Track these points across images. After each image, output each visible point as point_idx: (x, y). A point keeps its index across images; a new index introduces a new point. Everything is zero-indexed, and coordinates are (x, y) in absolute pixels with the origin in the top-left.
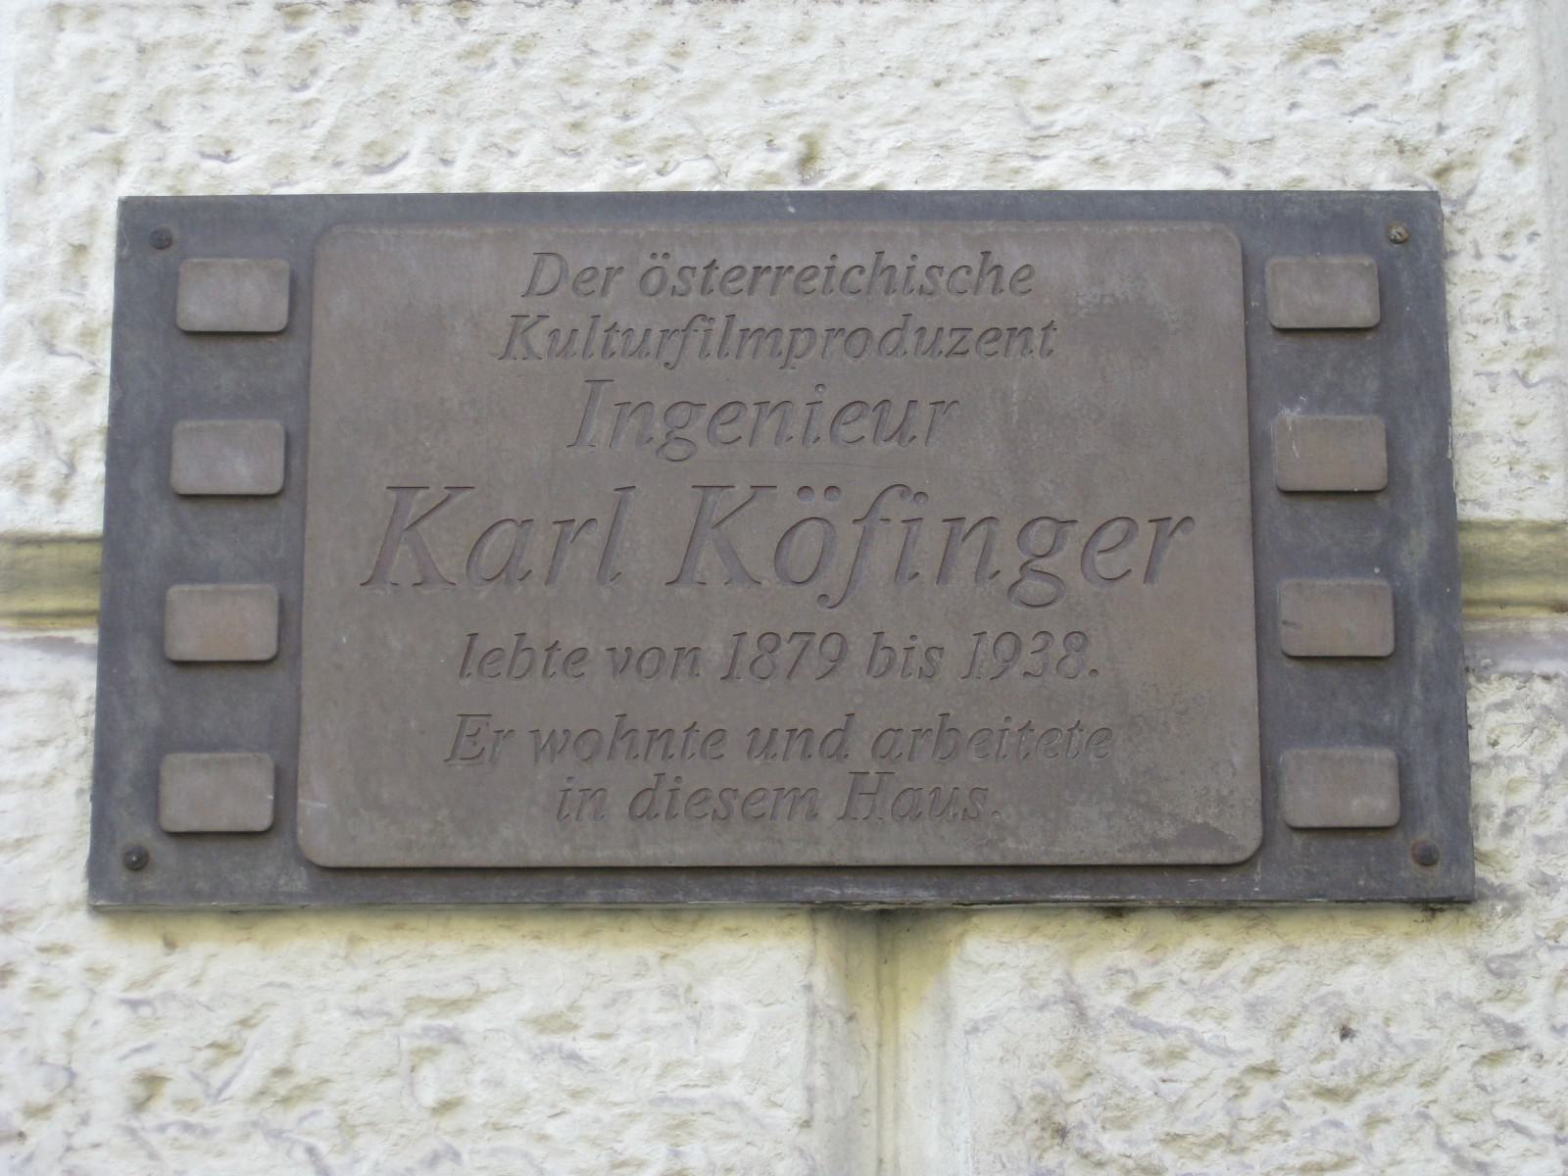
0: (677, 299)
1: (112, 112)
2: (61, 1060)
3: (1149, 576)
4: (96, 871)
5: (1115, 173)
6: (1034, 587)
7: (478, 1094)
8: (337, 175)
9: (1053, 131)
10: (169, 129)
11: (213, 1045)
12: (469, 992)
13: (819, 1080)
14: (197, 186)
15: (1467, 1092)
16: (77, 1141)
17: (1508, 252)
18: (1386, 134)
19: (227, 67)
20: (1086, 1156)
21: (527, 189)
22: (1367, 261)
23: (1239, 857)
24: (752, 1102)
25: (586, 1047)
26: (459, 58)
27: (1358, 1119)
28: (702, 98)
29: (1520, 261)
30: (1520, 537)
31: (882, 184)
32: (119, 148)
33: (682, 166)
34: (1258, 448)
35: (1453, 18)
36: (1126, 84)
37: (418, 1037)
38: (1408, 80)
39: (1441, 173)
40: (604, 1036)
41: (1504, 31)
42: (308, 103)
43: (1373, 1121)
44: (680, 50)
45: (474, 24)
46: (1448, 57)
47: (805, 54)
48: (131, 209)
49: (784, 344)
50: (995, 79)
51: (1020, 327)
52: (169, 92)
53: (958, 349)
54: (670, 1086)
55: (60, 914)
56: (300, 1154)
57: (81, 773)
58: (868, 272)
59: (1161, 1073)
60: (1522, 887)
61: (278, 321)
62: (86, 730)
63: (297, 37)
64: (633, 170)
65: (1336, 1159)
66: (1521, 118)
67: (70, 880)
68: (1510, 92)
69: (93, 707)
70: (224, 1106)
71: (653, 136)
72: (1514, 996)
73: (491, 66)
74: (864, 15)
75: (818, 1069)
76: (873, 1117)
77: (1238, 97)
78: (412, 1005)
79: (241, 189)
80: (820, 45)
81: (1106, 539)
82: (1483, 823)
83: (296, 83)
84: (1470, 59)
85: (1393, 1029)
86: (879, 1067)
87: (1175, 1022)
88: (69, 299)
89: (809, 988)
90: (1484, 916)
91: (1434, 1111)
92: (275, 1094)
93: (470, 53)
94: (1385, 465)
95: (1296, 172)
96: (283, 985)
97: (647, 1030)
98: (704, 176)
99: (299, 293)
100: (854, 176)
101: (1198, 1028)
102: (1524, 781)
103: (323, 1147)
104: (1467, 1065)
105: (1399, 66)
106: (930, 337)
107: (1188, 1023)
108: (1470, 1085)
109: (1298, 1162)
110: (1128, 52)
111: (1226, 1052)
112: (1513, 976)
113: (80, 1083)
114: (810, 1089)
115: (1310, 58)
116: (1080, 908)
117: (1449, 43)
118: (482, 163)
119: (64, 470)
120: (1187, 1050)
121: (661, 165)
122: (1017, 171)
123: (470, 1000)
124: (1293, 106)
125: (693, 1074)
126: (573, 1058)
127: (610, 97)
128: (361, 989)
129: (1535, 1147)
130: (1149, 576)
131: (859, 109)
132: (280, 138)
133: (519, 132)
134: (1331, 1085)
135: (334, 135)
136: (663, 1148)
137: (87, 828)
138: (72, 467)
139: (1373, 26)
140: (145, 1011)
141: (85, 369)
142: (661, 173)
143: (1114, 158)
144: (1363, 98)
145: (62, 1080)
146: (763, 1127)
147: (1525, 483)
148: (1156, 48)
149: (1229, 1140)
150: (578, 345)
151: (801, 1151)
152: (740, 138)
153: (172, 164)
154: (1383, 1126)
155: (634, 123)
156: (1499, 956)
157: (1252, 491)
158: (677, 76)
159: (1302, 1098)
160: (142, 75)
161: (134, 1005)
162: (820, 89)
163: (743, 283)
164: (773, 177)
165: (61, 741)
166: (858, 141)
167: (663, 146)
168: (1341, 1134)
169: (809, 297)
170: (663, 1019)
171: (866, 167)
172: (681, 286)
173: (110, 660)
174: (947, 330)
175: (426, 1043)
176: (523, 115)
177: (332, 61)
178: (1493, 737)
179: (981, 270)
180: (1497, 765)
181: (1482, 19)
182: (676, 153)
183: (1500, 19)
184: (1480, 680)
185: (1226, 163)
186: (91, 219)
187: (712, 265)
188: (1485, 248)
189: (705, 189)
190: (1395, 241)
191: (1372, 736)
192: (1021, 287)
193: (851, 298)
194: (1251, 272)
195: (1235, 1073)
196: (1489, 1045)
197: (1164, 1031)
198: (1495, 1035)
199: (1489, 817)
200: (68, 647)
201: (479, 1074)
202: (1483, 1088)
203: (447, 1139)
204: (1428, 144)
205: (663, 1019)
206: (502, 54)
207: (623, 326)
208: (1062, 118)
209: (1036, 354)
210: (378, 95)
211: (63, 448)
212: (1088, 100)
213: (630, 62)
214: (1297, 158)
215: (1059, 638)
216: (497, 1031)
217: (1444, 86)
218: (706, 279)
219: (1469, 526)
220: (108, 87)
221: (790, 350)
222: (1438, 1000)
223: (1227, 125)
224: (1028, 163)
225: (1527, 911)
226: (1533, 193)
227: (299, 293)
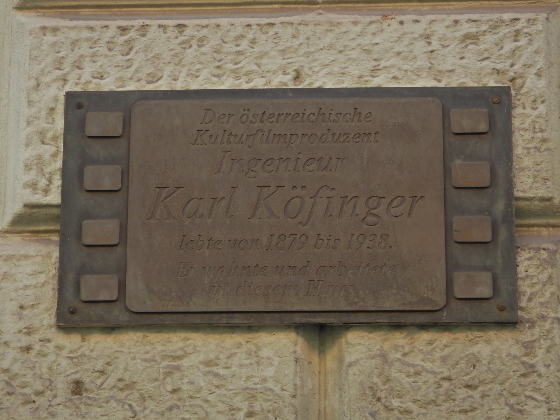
8: (138, 84)
28: (261, 57)
31: (321, 86)
44: (253, 41)
47: (297, 42)
64: (238, 82)
71: (245, 70)
74: (316, 29)
80: (301, 39)
98: (262, 83)
100: (312, 83)
118: (187, 80)
122: (367, 81)
127: (230, 57)
131: (314, 61)
141: (54, 149)
142: (247, 82)
164: (285, 84)
166: (313, 72)
171: (316, 80)
172: (253, 120)
176: (201, 63)
182: (252, 76)
189: (262, 88)
193: (310, 124)
208: (383, 63)
211: (47, 176)
213: (237, 45)
218: (262, 117)
224: (371, 78)
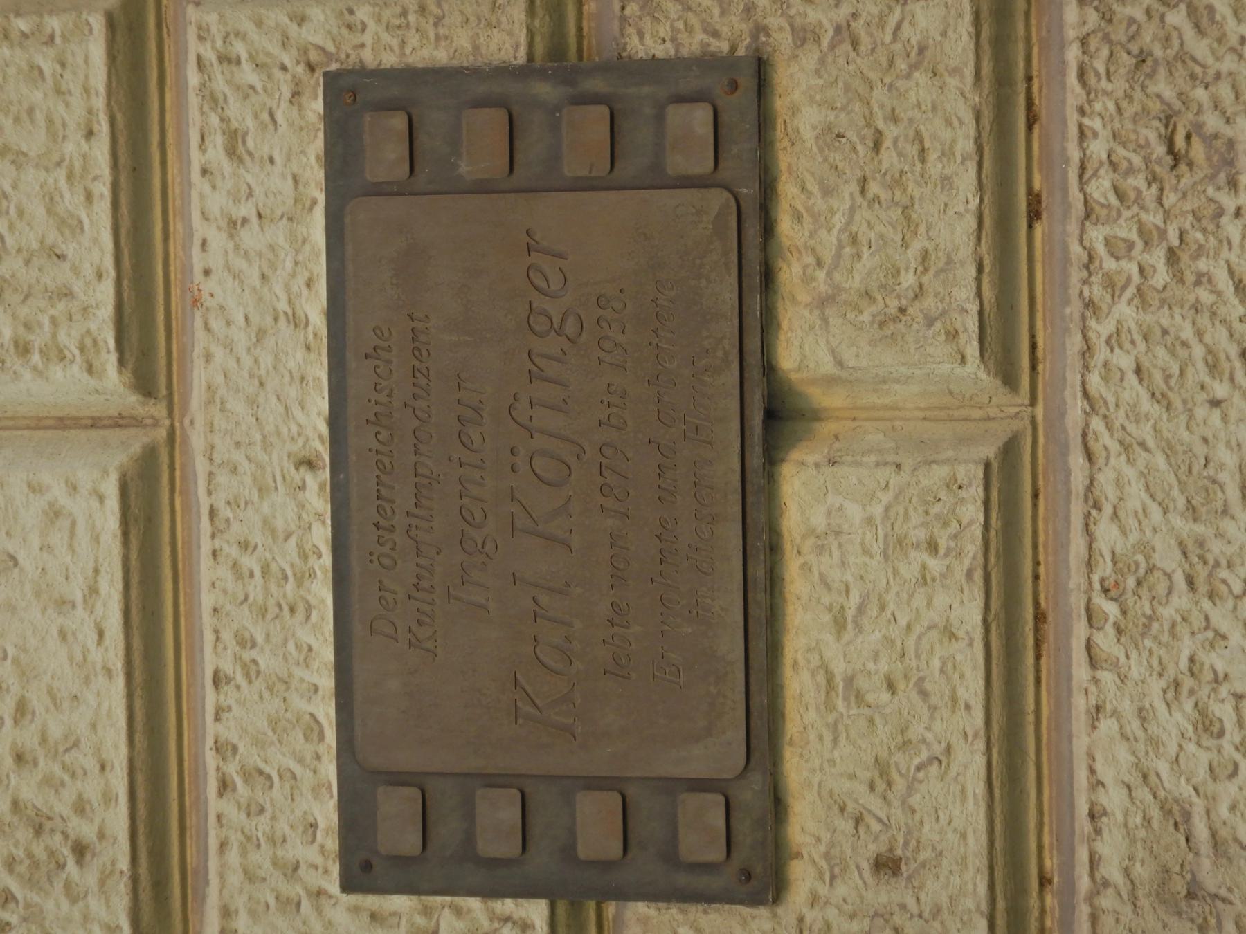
0: (397, 547)
1: (288, 899)
2: (867, 921)
3: (561, 256)
4: (755, 900)
5: (315, 274)
6: (571, 327)
7: (884, 666)
8: (325, 759)
9: (290, 313)
10: (298, 862)
11: (856, 829)
12: (822, 672)
13: (873, 458)
14: (333, 844)
15: (875, 60)
16: (915, 911)
17: (359, 27)
18: (288, 104)
19: (260, 826)
20: (916, 296)
21: (331, 639)
22: (368, 118)
23: (733, 203)
24: (886, 498)
25: (855, 599)
26: (250, 682)
27: (893, 128)
28: (273, 532)
29: (365, 19)
30: (537, 23)
31: (325, 419)
32: (309, 893)
33: (316, 543)
34: (483, 188)
35: (214, 59)
36: (260, 267)
37: (849, 704)
38: (252, 87)
39: (311, 68)
40: (847, 591)
41: (221, 27)
42: (281, 777)
43: (894, 118)
44: (244, 546)
45: (230, 673)
46: (238, 62)
47: (245, 466)
48: (348, 886)
49: (426, 481)
50: (259, 350)
51: (412, 335)
52: (275, 863)
53: (426, 374)
54: (877, 548)
55: (779, 923)
56: (921, 775)
57: (695, 911)
58: (378, 429)
59: (865, 249)
60: (751, 24)
61: (414, 792)
62: (668, 908)
63: (239, 781)
64: (319, 573)
65: (917, 142)
66: (277, 17)
67: (761, 915)
68: (259, 24)
69: (653, 905)
70: (893, 822)
71: (297, 561)
72: (817, 30)
73: (254, 662)
74: (220, 430)
75: (866, 459)
76: (897, 423)
77: (266, 196)
78: (830, 707)
79: (335, 818)
80: (238, 457)
81: (541, 283)
82: (712, 48)
83: (268, 784)
84: (239, 48)
85: (839, 105)
86: (867, 420)
87: (834, 240)
88: (403, 922)
89: (817, 465)
90: (769, 49)
91: (887, 80)
92: (885, 790)
93: (247, 676)
94: (493, 109)
95: (313, 159)
96: (819, 785)
97: (843, 563)
98: (322, 529)
99: (397, 779)
100: (321, 437)
101: (838, 226)
102: (686, 23)
103: (916, 761)
104: (859, 60)
105: (247, 92)
106: (417, 391)
107: (835, 231)
108: (871, 58)
109: (919, 165)
110: (239, 263)
111: (852, 210)
112: (805, 30)
113: (881, 910)
114: (877, 464)
115: (241, 149)
116: (766, 300)
117: (229, 61)
118: (316, 667)
119: (509, 925)
120: (851, 234)
121: (315, 556)
122: (315, 335)
123: (826, 672)
124: (271, 160)
125: (869, 536)
126: (861, 610)
127: (273, 588)
128: (821, 738)
129: (909, 18)
130: (561, 256)
131: (278, 434)
132: (301, 794)
133: (296, 645)
134: (872, 145)
135: (301, 761)
136: (913, 554)
137: (727, 907)
138: (507, 919)
139: (220, 110)
140: (837, 870)
141: (447, 911)
142: (320, 557)
143: (307, 274)
144: (265, 116)
145: (879, 921)
146: (900, 493)
147: (504, 19)
148: (237, 247)
149: (905, 208)
150: (427, 608)
151: (915, 469)
152: (297, 506)
153: (319, 860)
154: (897, 112)
155: (289, 573)
156: (793, 39)
157: (510, 192)
158: (260, 545)
159: (880, 162)
160: (264, 880)
161: (833, 877)
162: (267, 458)
163: (387, 506)
164: (322, 487)
165: (675, 924)
166: (299, 435)
167: (304, 556)
168: (902, 139)
169: (395, 466)
170: (836, 553)
171: (315, 429)
172: (389, 545)
173: (624, 895)
174: (415, 381)
175: (853, 699)
176: (285, 641)
177: (254, 759)
178: (659, 41)
179: (377, 359)
180: (676, 39)
181: (213, 41)
182: (308, 547)
183: (214, 29)
184: (625, 49)
185: (308, 204)
186: (355, 910)
187: (377, 526)
188: (357, 41)
189: (330, 529)
190: (355, 99)
191: (660, 118)
192: (386, 334)
193: (396, 440)
194: (378, 190)
195: (865, 204)
196: (847, 46)
197: (840, 247)
198: (841, 42)
199: (708, 45)
200: (619, 919)
201: (871, 666)
202: (873, 50)
203: (911, 685)
204: (294, 77)
205: (836, 553)
206: (247, 655)
207: (415, 581)
208: (283, 306)
209: (428, 325)
210: (275, 733)
211: (496, 925)
212: (270, 290)
213: (252, 575)
214: (304, 159)
215: (601, 312)
216: (845, 655)
217: (257, 65)
218: (385, 529)
219: (531, 57)
220: (272, 902)
221: (427, 477)
222: (820, 77)
223: (284, 203)
224: (310, 329)
225: (767, 21)
226: (323, 11)
227: (397, 779)
